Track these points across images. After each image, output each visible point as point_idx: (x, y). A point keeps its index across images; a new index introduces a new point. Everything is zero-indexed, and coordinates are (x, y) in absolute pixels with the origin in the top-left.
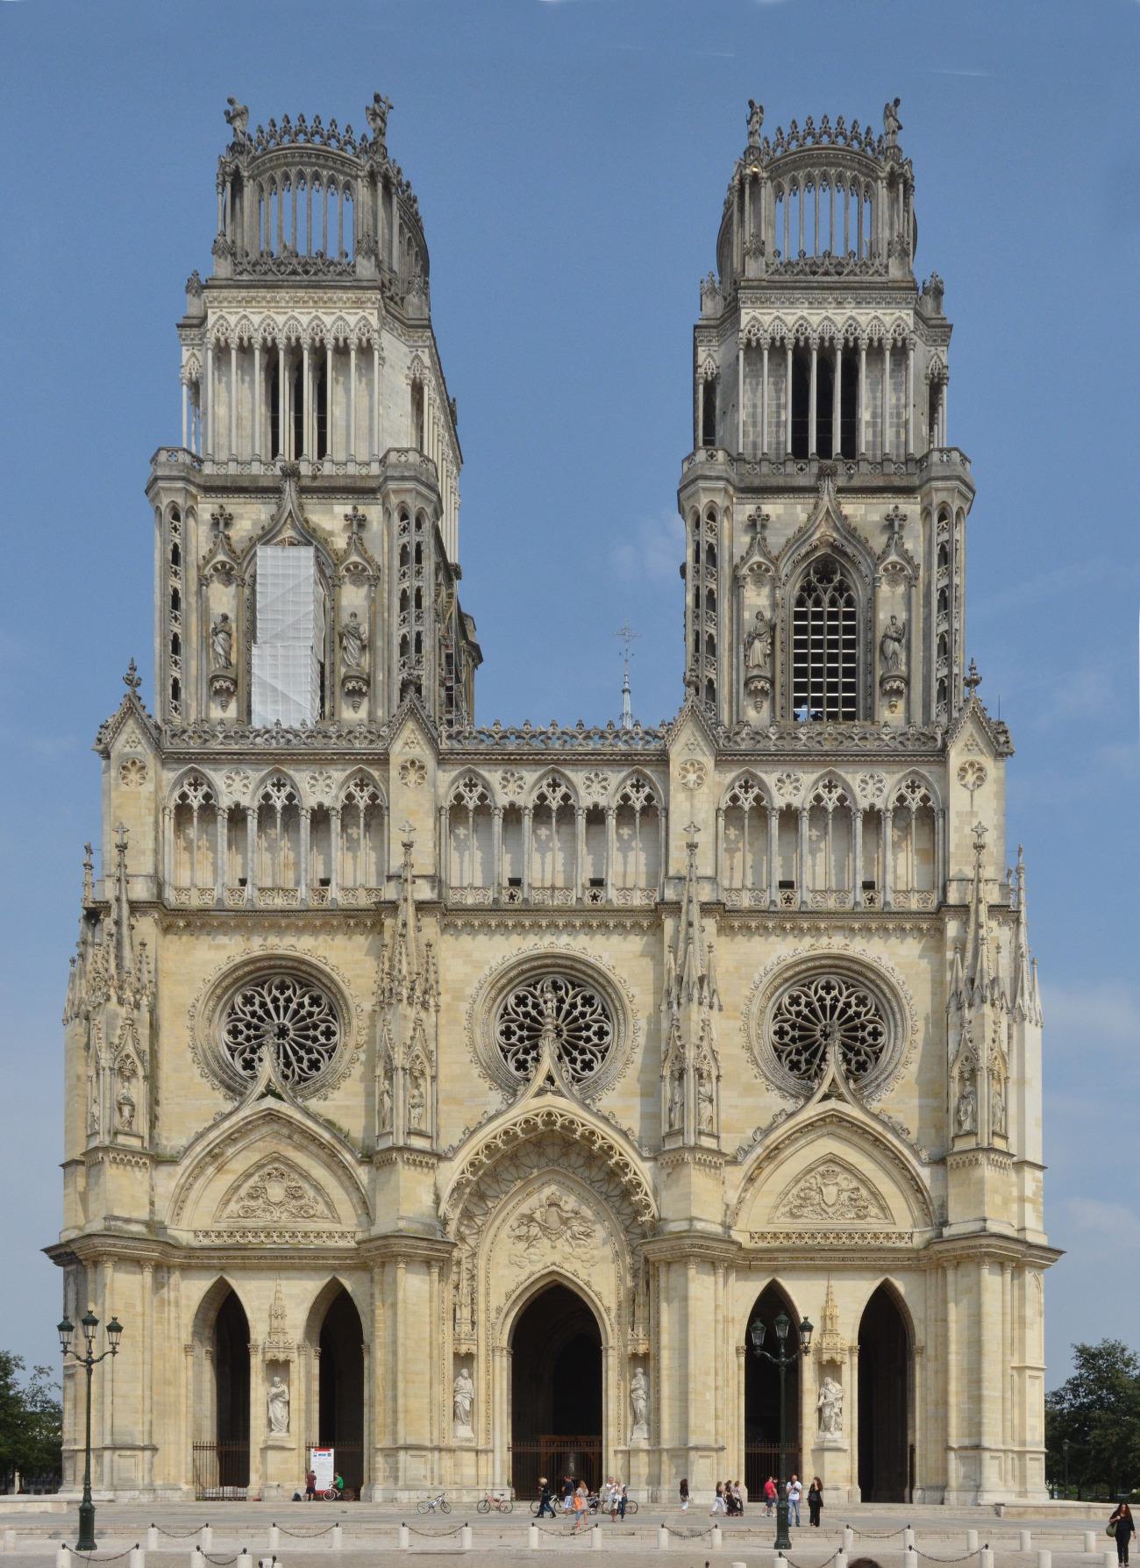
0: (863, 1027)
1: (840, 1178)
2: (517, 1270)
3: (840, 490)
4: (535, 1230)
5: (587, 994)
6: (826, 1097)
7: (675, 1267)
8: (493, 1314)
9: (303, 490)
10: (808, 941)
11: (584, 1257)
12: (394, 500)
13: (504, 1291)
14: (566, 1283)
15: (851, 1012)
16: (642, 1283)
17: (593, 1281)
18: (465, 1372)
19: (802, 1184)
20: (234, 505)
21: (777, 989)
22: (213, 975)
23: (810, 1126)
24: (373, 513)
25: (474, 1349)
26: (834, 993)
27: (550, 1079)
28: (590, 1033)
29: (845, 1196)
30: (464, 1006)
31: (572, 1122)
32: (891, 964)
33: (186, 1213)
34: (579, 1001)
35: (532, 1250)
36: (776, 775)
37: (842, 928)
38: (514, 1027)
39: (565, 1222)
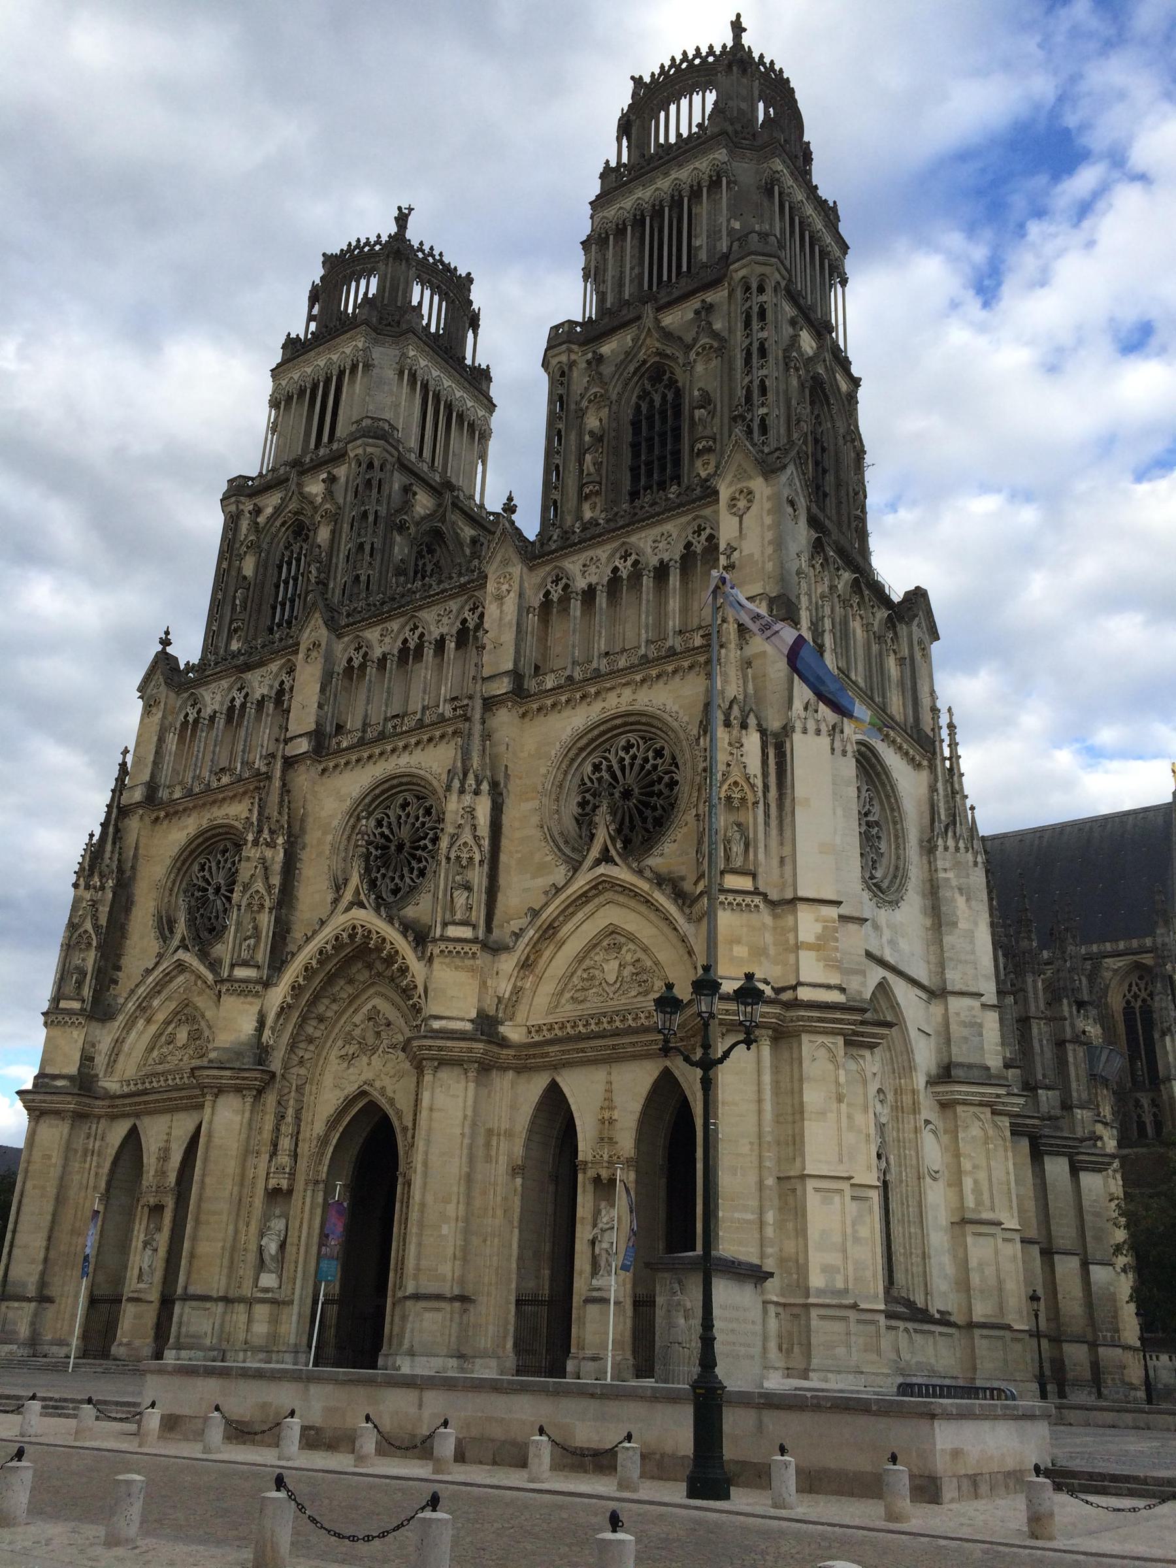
0: (660, 779)
1: (624, 949)
2: (337, 1092)
3: (659, 309)
6: (598, 862)
9: (302, 473)
10: (597, 706)
12: (352, 455)
15: (648, 766)
19: (588, 963)
20: (260, 501)
21: (573, 760)
22: (175, 850)
23: (584, 898)
24: (341, 472)
26: (633, 751)
29: (626, 973)
30: (329, 838)
32: (675, 708)
33: (119, 1066)
35: (351, 1070)
36: (581, 562)
37: (627, 684)
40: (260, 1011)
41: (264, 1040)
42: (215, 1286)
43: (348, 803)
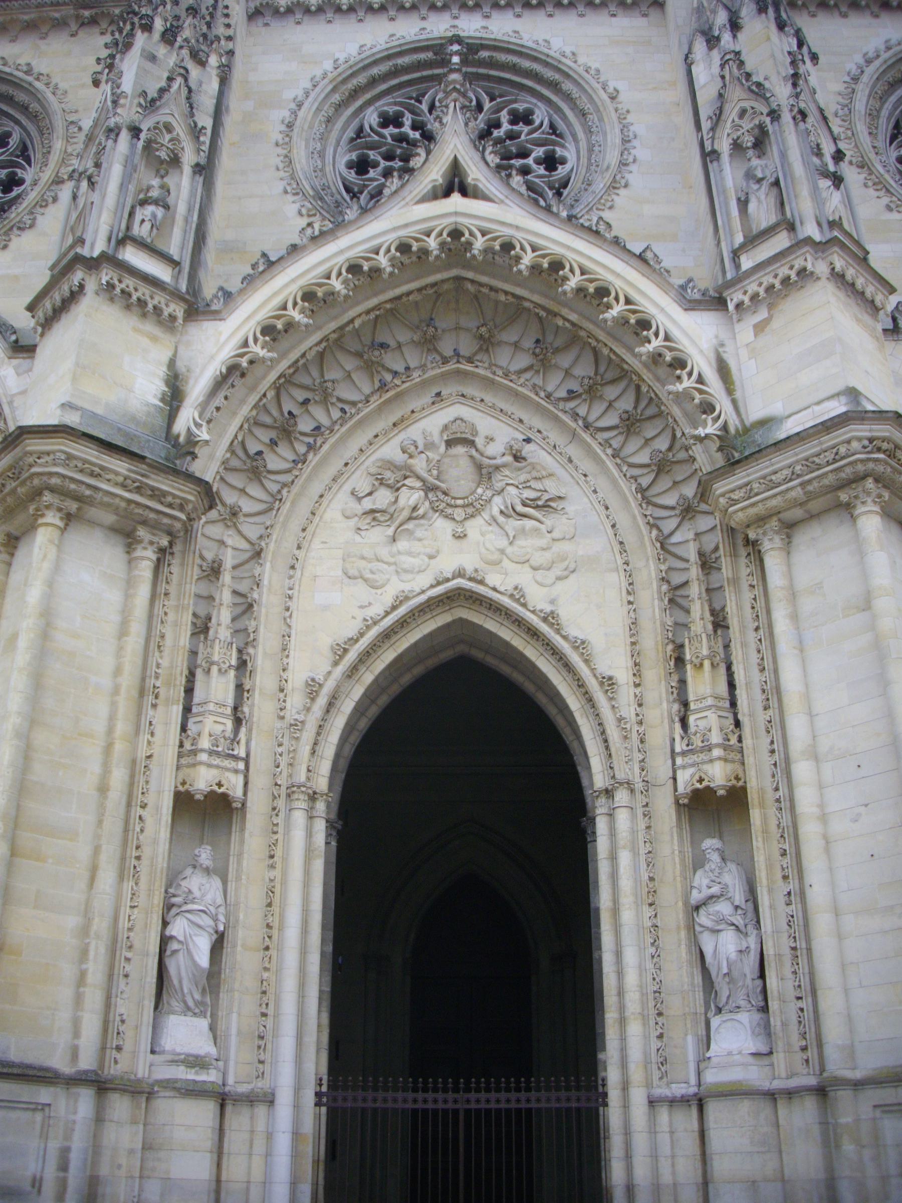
4: (410, 497)
5: (521, 107)
7: (802, 538)
8: (295, 701)
11: (539, 558)
13: (325, 641)
14: (491, 625)
16: (698, 611)
17: (565, 614)
18: (205, 855)
25: (234, 785)
27: (456, 168)
28: (530, 161)
31: (507, 247)
34: (504, 116)
35: (403, 544)
38: (373, 155)
39: (485, 472)
40: (172, 363)
41: (181, 425)
42: (63, 1039)
43: (328, 65)
